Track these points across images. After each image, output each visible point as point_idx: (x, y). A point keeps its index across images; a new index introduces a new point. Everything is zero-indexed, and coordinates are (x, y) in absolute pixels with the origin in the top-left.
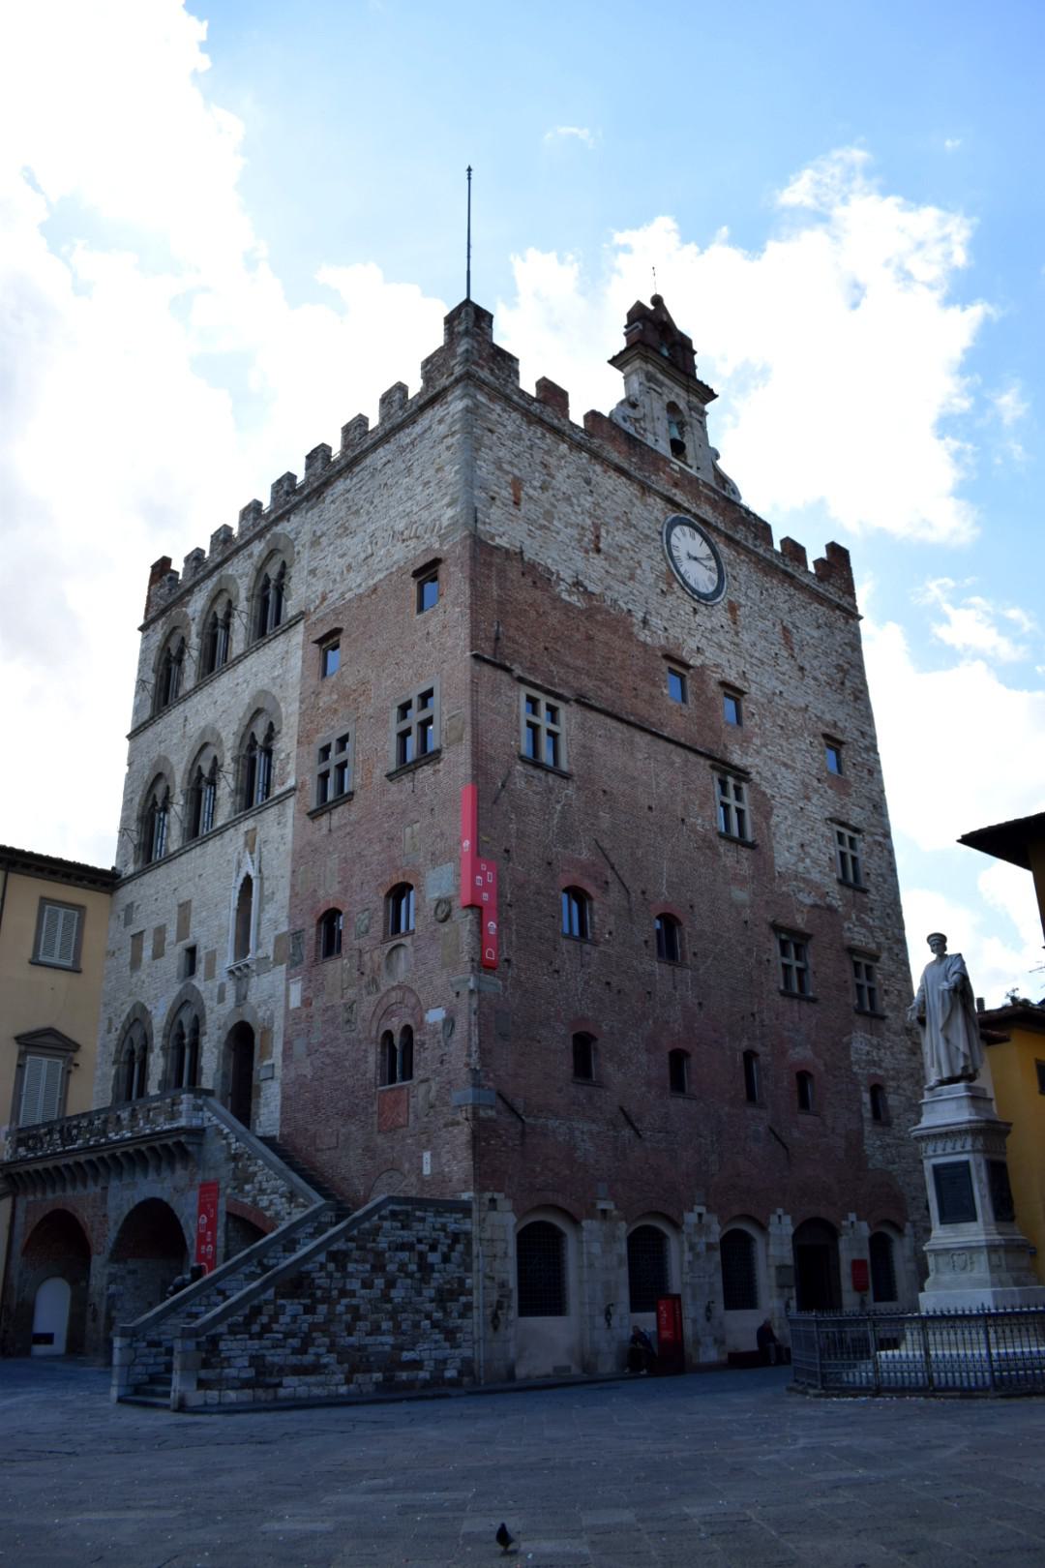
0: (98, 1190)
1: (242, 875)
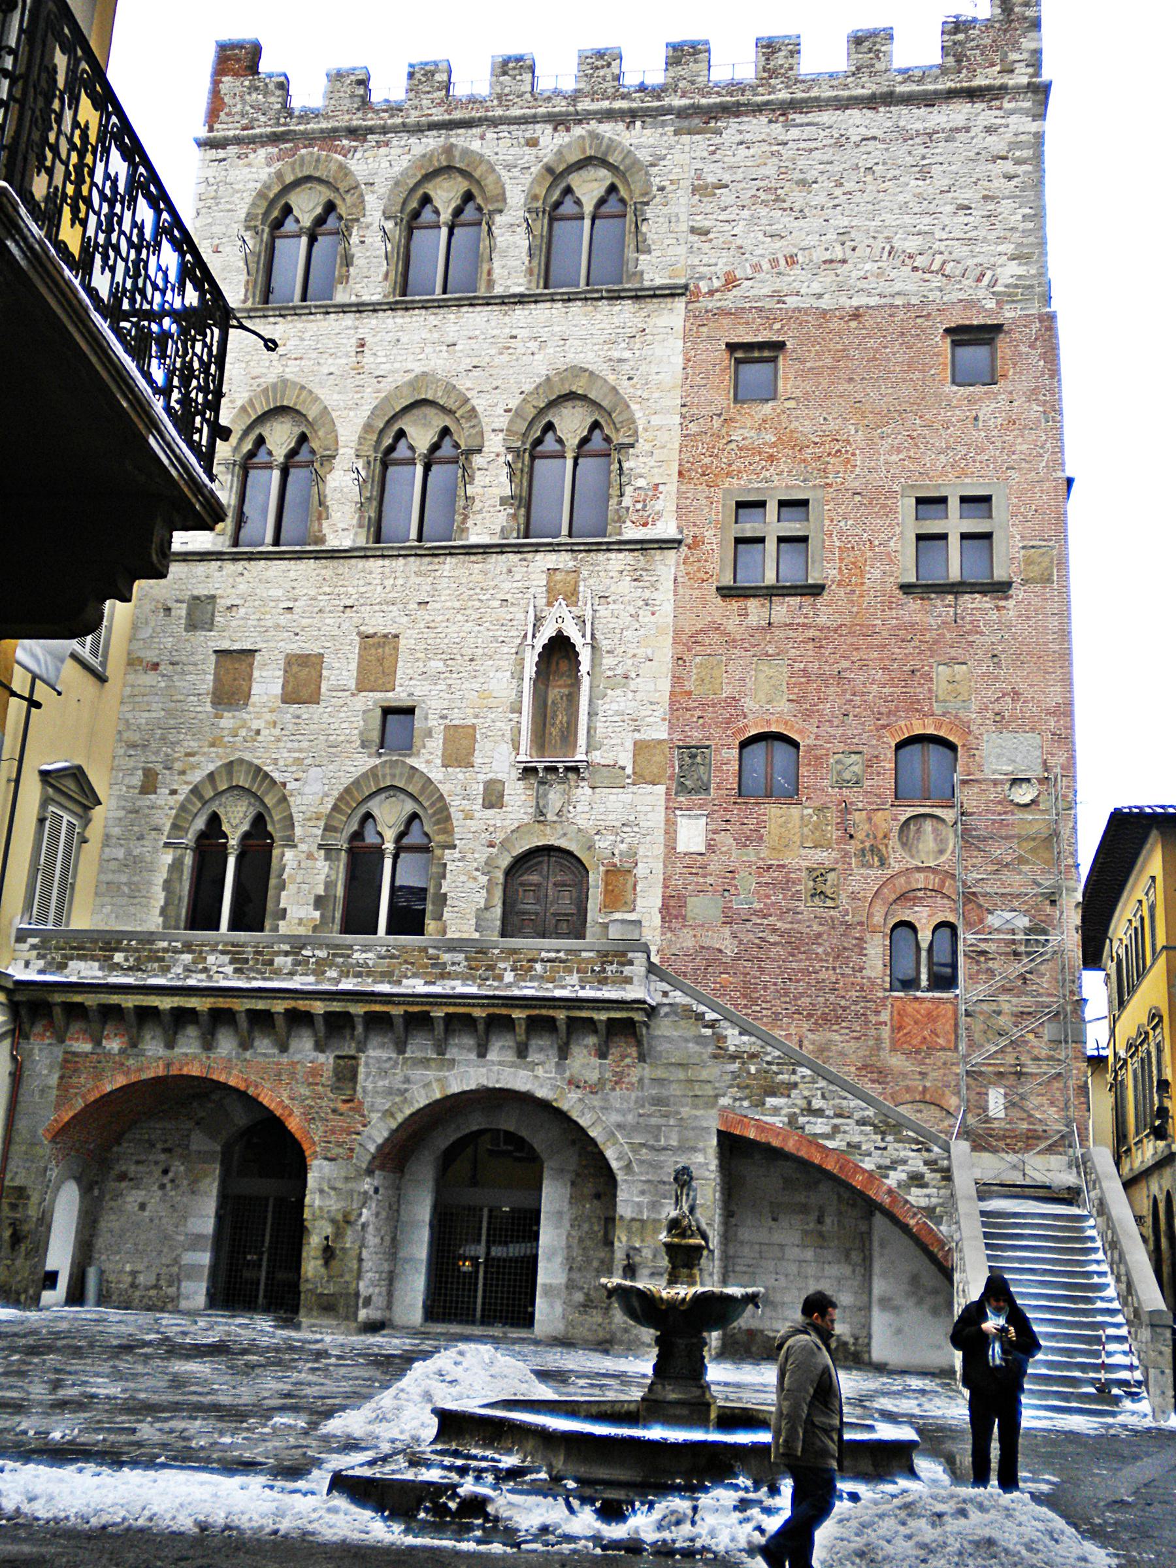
0: (326, 1060)
1: (547, 632)
